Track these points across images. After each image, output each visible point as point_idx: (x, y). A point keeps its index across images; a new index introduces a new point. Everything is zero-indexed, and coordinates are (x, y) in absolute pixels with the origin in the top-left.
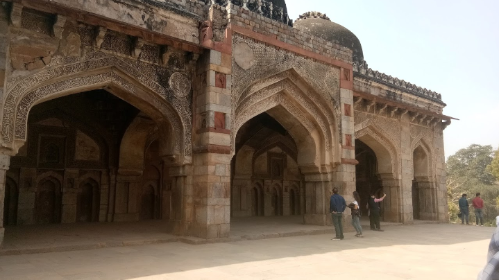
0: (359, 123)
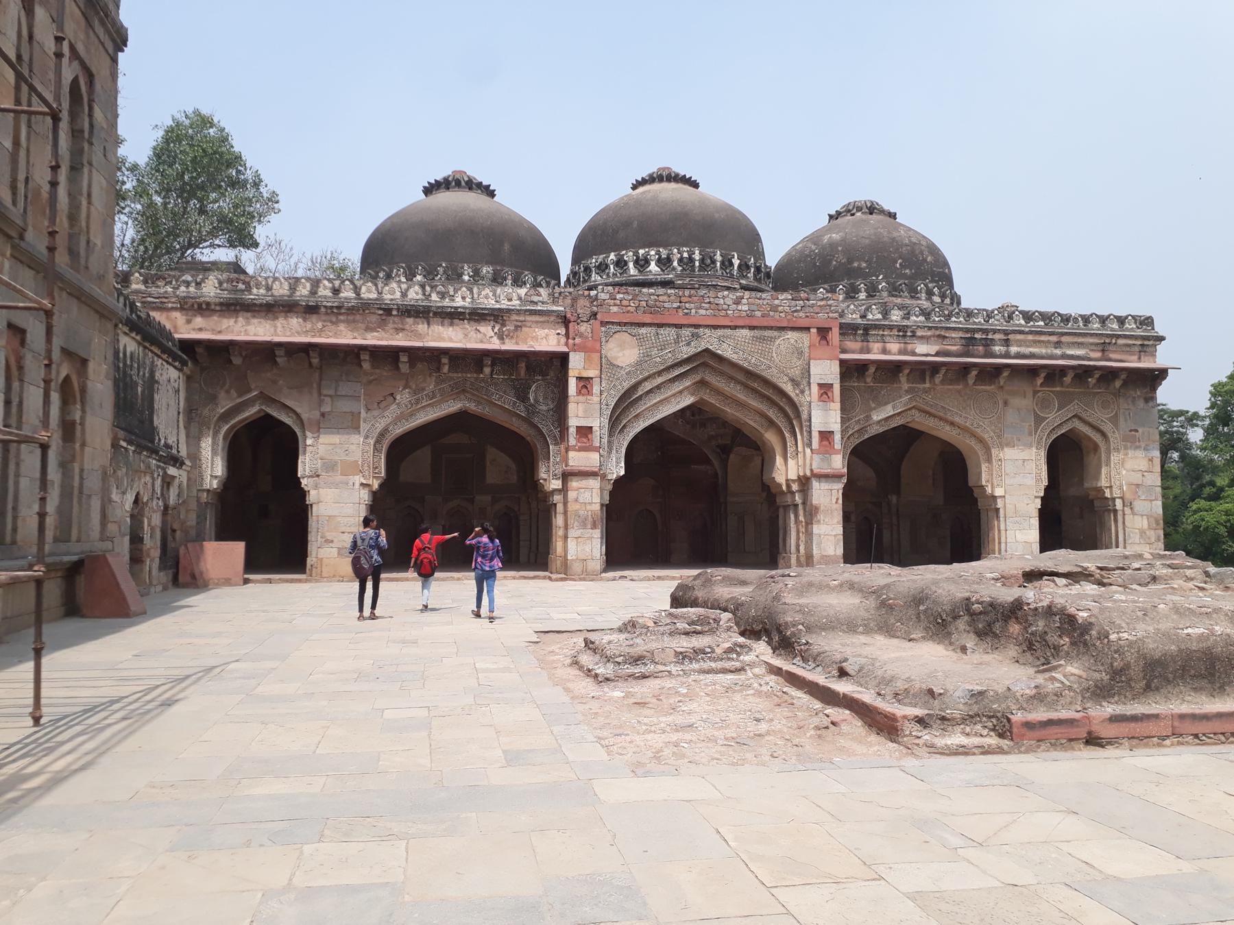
0: (886, 404)
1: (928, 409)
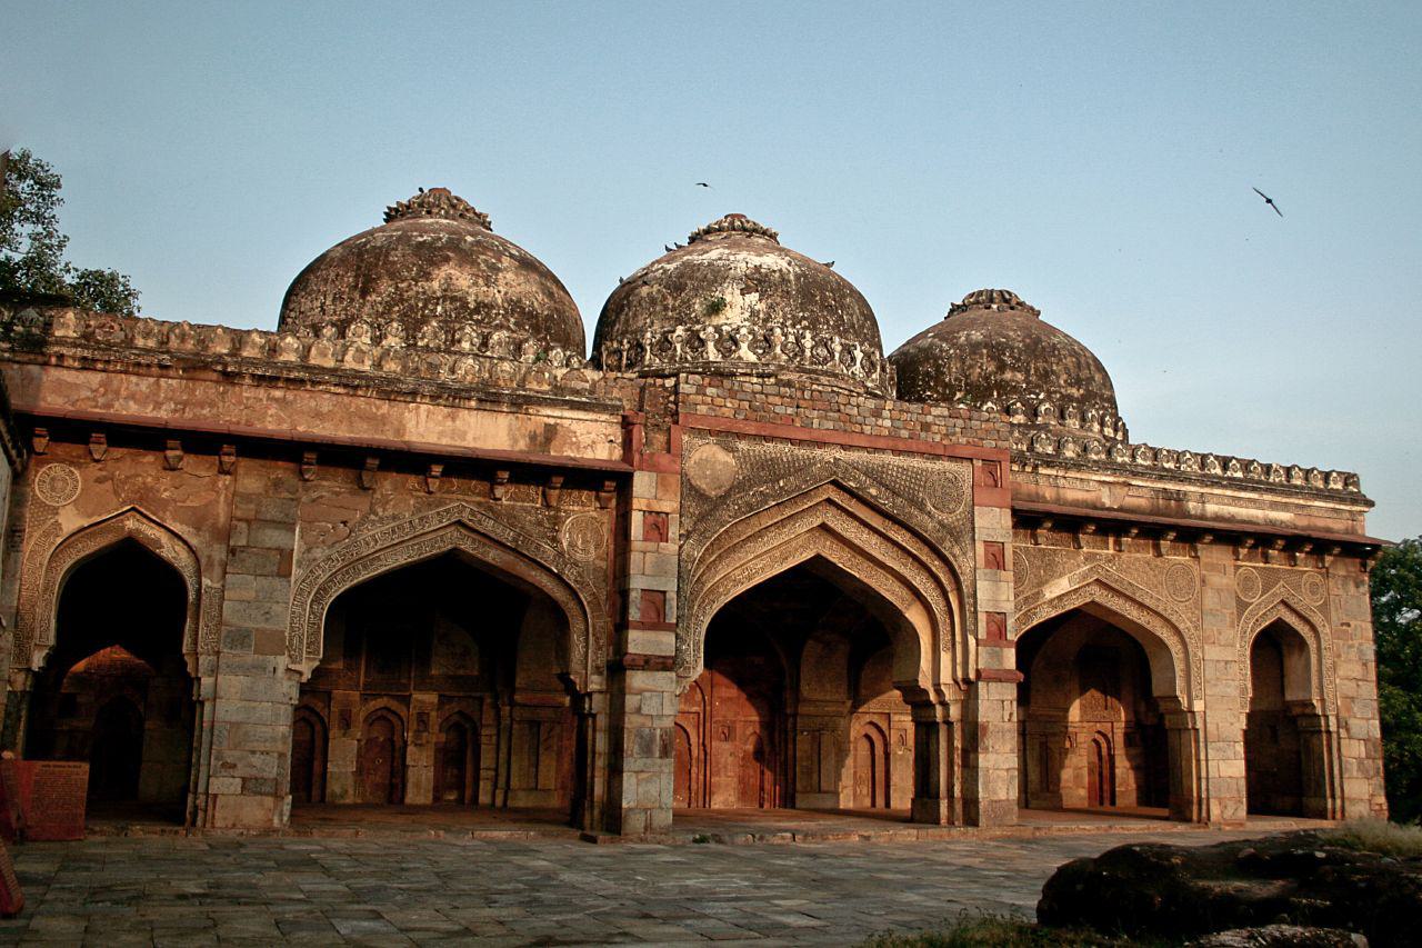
0: (1060, 576)
1: (1113, 585)
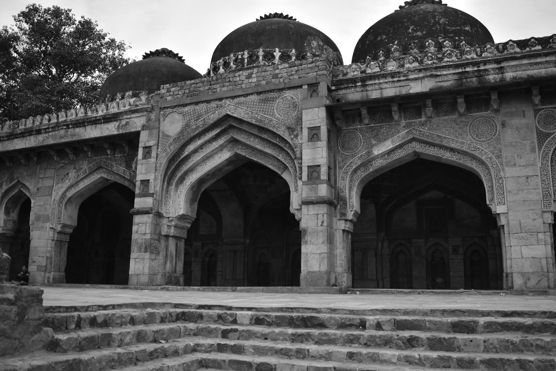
0: (385, 140)
1: (425, 139)
